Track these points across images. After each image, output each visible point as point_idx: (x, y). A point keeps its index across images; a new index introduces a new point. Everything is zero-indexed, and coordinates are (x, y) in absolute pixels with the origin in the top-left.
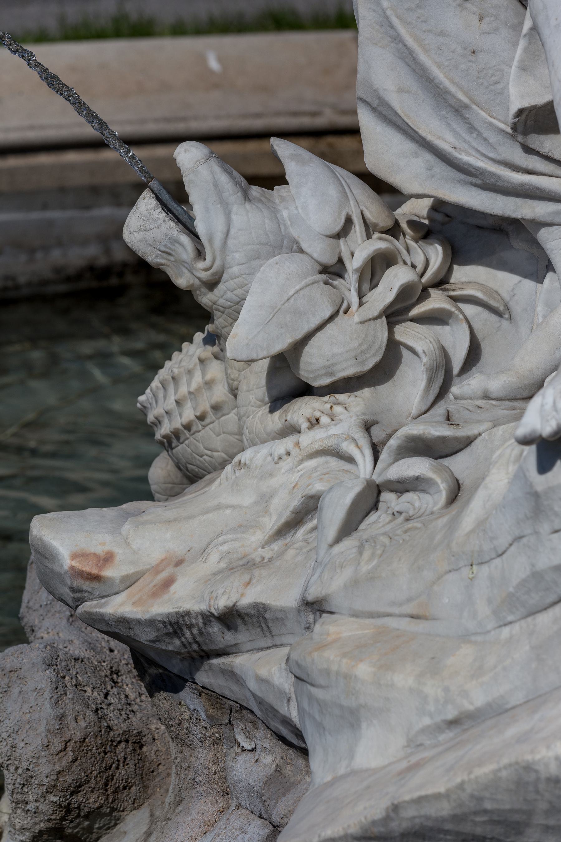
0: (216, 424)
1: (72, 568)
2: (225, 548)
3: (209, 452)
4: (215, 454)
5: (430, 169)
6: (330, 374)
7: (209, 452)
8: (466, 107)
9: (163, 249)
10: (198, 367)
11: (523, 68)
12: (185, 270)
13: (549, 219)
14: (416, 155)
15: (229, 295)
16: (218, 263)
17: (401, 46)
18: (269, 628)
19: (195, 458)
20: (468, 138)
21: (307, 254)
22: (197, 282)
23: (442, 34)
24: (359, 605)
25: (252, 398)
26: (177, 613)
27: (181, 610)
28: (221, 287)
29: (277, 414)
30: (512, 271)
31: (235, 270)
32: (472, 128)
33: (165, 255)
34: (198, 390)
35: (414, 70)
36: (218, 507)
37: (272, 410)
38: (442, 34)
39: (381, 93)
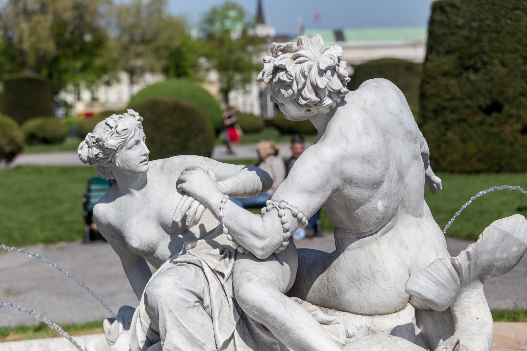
8: (204, 344)
11: (219, 328)
38: (194, 322)
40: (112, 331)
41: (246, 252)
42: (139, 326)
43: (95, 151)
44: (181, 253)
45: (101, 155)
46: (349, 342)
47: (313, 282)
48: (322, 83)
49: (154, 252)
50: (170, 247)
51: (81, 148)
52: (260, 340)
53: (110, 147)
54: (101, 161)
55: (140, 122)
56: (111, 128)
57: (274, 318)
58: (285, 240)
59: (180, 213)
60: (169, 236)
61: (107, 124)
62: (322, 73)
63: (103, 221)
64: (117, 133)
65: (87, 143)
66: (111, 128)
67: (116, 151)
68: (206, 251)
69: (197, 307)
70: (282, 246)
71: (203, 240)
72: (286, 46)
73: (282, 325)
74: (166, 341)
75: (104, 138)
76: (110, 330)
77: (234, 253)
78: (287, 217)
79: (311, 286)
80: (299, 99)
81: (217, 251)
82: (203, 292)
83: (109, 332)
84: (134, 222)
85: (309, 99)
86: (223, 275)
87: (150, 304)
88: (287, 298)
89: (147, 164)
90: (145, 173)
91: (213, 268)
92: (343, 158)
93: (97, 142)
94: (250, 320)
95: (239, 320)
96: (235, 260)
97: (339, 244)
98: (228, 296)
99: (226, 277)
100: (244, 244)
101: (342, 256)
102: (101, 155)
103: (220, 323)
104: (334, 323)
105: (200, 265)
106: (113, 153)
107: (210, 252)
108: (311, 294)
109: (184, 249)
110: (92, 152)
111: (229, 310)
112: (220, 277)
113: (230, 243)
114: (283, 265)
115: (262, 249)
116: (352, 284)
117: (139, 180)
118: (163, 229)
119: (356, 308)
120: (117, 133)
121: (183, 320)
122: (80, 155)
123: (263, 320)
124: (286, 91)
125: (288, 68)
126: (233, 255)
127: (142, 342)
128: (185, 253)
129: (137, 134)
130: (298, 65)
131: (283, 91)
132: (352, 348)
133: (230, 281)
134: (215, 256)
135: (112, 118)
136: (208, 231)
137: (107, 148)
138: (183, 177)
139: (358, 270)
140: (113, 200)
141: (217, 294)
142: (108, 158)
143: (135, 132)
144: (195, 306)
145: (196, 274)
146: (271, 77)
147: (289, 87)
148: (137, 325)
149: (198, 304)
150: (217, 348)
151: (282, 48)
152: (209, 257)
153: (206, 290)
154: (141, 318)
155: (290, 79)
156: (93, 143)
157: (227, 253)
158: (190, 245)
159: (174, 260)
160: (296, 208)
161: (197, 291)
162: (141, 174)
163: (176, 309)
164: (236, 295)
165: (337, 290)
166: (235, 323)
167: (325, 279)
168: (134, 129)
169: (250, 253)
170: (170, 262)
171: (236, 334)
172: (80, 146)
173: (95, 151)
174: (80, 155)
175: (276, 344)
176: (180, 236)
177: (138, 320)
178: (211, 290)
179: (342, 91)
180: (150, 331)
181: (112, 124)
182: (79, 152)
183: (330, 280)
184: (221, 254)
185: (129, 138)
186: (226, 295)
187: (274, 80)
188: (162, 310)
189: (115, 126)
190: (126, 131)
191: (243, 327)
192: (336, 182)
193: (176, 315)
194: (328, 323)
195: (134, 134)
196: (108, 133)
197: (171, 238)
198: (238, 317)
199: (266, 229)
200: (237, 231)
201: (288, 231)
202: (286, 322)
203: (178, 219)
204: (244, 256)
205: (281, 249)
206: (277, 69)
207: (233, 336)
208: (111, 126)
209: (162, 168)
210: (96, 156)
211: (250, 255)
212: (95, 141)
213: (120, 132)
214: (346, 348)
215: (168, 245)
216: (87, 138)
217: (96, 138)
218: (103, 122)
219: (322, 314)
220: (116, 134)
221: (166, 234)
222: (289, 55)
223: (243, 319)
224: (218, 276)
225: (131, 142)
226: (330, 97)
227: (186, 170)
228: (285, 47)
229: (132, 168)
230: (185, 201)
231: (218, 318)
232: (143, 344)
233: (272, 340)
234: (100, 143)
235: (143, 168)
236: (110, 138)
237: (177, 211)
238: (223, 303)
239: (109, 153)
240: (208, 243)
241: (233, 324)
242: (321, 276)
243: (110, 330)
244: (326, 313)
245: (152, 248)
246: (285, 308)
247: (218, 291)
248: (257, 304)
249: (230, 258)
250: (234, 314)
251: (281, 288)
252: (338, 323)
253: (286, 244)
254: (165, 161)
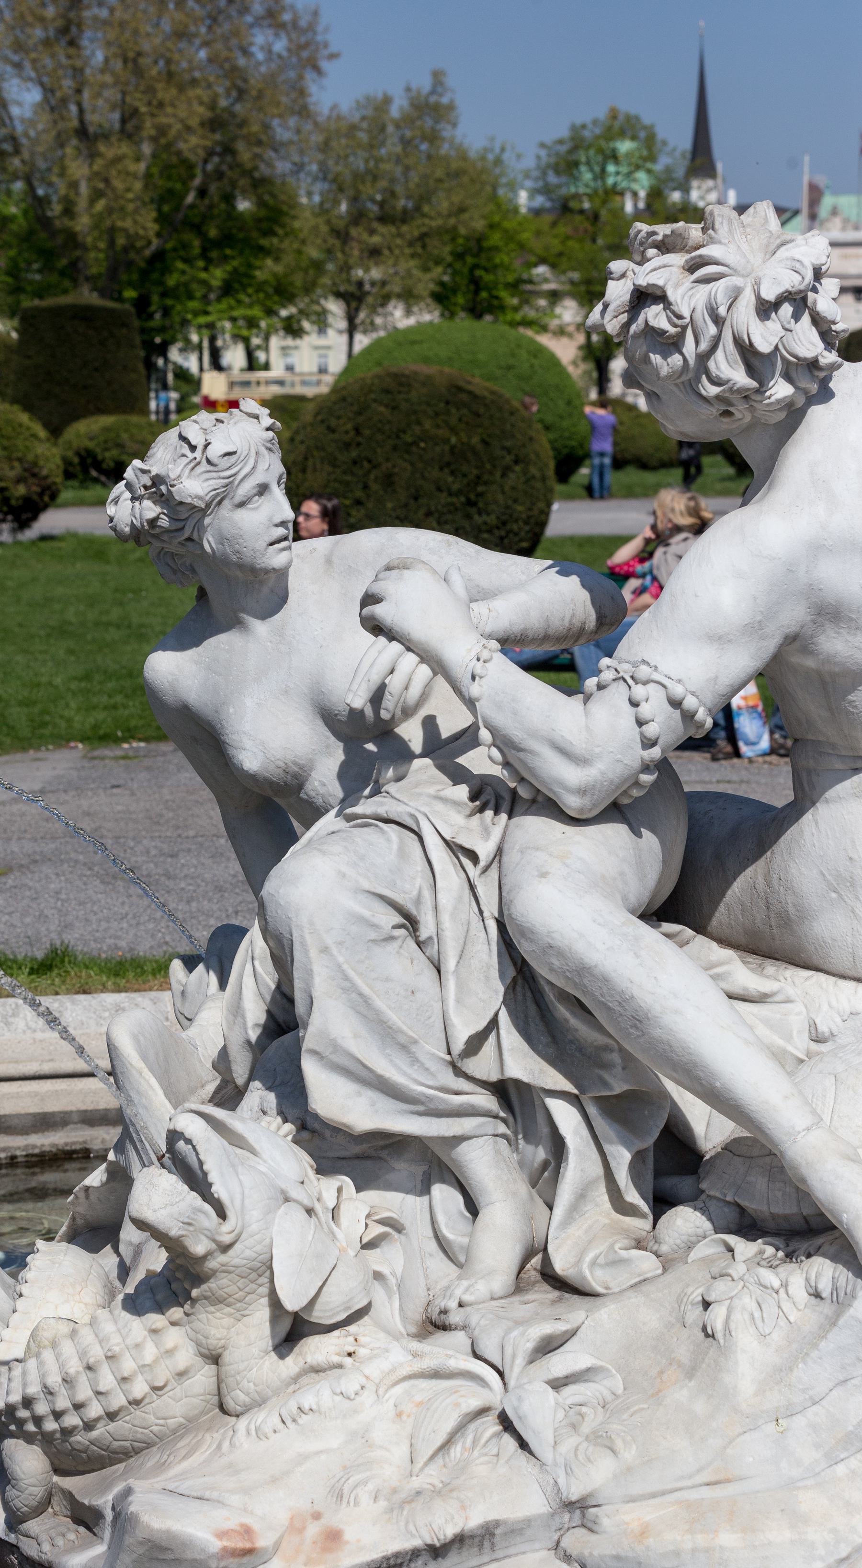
0: (178, 1389)
1: (225, 1549)
2: (370, 1486)
3: (162, 1422)
4: (169, 1421)
5: (373, 1105)
6: (349, 1308)
7: (162, 1422)
8: (415, 1042)
9: (186, 1220)
10: (149, 1339)
11: (458, 1001)
12: (203, 1238)
13: (472, 1134)
14: (359, 1094)
15: (248, 1253)
16: (240, 1224)
17: (354, 995)
18: (493, 1544)
19: (137, 1432)
20: (410, 1071)
21: (295, 1201)
22: (214, 1246)
23: (387, 980)
24: (637, 1489)
25: (255, 1351)
26: (384, 1557)
27: (390, 1552)
28: (237, 1246)
29: (289, 1360)
30: (397, 1190)
31: (254, 1227)
32: (414, 1060)
33: (186, 1226)
34: (156, 1361)
35: (365, 1017)
36: (303, 1458)
37: (282, 1357)
38: (387, 980)
39: (339, 1041)
40: (190, 989)
41: (540, 798)
42: (249, 982)
43: (150, 509)
44: (367, 792)
45: (164, 522)
46: (818, 1054)
47: (728, 884)
48: (764, 336)
49: (301, 787)
50: (343, 774)
51: (116, 501)
52: (570, 1037)
53: (189, 500)
54: (165, 537)
55: (271, 434)
56: (193, 448)
57: (606, 980)
58: (646, 768)
59: (364, 686)
60: (341, 745)
61: (183, 438)
62: (766, 309)
63: (169, 699)
64: (209, 462)
65: (129, 486)
66: (193, 448)
67: (203, 512)
68: (432, 790)
69: (399, 942)
70: (637, 784)
71: (427, 761)
72: (668, 232)
73: (625, 1000)
74: (311, 1029)
75: (173, 475)
76: (185, 986)
77: (507, 797)
78: (654, 706)
79: (723, 895)
80: (699, 380)
81: (462, 792)
82: (418, 901)
83: (183, 993)
84: (249, 703)
85: (728, 381)
86: (474, 857)
87: (271, 927)
88: (643, 928)
89: (289, 548)
90: (282, 574)
91: (448, 837)
92: (817, 549)
93: (154, 484)
94: (542, 982)
95: (514, 980)
96: (510, 816)
97: (802, 785)
98: (486, 914)
99: (483, 863)
100: (535, 775)
101: (808, 817)
102: (164, 522)
103: (460, 986)
104: (776, 999)
105: (416, 828)
106: (197, 516)
107: (442, 794)
108: (721, 917)
109: (377, 782)
110: (141, 510)
111: (485, 953)
112: (466, 862)
113: (496, 771)
114: (639, 835)
115: (582, 791)
116: (834, 895)
117: (265, 590)
118: (327, 725)
119: (841, 961)
120: (209, 462)
121: (360, 974)
122: (111, 520)
123: (575, 984)
124: (665, 358)
125: (671, 295)
126: (506, 805)
127: (257, 1025)
128: (376, 792)
129: (263, 466)
130: (702, 286)
131: (656, 358)
132: (821, 1072)
133: (494, 873)
134: (456, 803)
135: (195, 422)
136: (445, 734)
137: (181, 503)
138: (377, 589)
139: (851, 859)
140: (197, 644)
141: (455, 908)
142: (182, 528)
143: (256, 461)
144: (392, 938)
145: (402, 853)
146: (624, 318)
147: (672, 348)
148: (245, 979)
149: (403, 932)
150: (450, 1054)
151: (659, 237)
152: (439, 806)
153: (427, 894)
154: (257, 963)
155: (675, 326)
156: (146, 487)
157: (488, 796)
158: (390, 773)
159: (349, 811)
160: (679, 681)
161: (399, 898)
162: (273, 576)
163: (341, 943)
164: (506, 913)
165: (791, 910)
166: (501, 989)
167: (761, 879)
168: (253, 454)
169: (550, 799)
170: (337, 815)
171: (504, 1018)
172: (112, 496)
173: (150, 509)
174: (111, 520)
175: (612, 1051)
176: (371, 747)
177: (249, 966)
178: (439, 896)
179: (823, 361)
180: (279, 997)
181: (196, 438)
182: (111, 510)
183: (775, 882)
184: (473, 798)
185: (239, 477)
186: (481, 912)
187: (633, 328)
188: (303, 944)
189: (203, 442)
190: (233, 458)
191: (525, 1000)
192: (793, 616)
193: (341, 959)
194: (761, 999)
195: (254, 468)
196: (185, 461)
197: (346, 751)
198: (511, 972)
199: (592, 735)
200: (516, 739)
201: (654, 744)
202: (636, 992)
203: (359, 700)
204: (534, 807)
205: (636, 793)
206: (643, 297)
207: (494, 1023)
208: (193, 443)
209: (329, 561)
210: (153, 522)
211: (548, 806)
212: (149, 483)
213: (215, 460)
214: (805, 1069)
215: (336, 769)
216: (129, 473)
217: (153, 473)
218: (172, 435)
219: (742, 973)
220: (204, 467)
221: (333, 739)
222: (677, 259)
223: (525, 979)
224: (463, 859)
225: (246, 489)
226: (788, 377)
227: (388, 568)
228: (665, 236)
229: (248, 556)
230: (380, 652)
231: (456, 971)
232: (259, 1031)
233: (601, 1040)
234: (163, 488)
235: (276, 559)
236: (189, 477)
237: (358, 680)
238: (472, 932)
239: (186, 517)
240: (441, 768)
241: (496, 992)
242: (749, 871)
243: (185, 986)
244: (760, 970)
245: (295, 776)
246: (637, 956)
247: (460, 899)
248: (558, 940)
249: (497, 812)
250: (500, 963)
251: (633, 899)
252: (788, 1001)
253: (647, 778)
254: (337, 543)
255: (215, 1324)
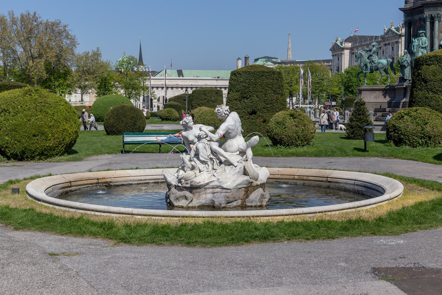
78: (219, 135)
192: (227, 129)
199: (216, 136)
206: (218, 110)
211: (213, 141)
255: (195, 171)
